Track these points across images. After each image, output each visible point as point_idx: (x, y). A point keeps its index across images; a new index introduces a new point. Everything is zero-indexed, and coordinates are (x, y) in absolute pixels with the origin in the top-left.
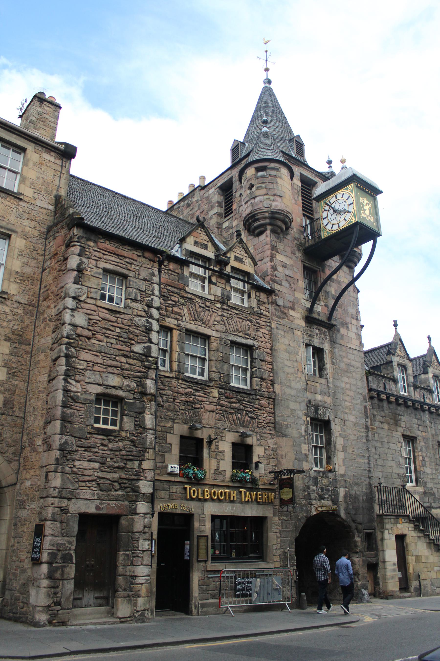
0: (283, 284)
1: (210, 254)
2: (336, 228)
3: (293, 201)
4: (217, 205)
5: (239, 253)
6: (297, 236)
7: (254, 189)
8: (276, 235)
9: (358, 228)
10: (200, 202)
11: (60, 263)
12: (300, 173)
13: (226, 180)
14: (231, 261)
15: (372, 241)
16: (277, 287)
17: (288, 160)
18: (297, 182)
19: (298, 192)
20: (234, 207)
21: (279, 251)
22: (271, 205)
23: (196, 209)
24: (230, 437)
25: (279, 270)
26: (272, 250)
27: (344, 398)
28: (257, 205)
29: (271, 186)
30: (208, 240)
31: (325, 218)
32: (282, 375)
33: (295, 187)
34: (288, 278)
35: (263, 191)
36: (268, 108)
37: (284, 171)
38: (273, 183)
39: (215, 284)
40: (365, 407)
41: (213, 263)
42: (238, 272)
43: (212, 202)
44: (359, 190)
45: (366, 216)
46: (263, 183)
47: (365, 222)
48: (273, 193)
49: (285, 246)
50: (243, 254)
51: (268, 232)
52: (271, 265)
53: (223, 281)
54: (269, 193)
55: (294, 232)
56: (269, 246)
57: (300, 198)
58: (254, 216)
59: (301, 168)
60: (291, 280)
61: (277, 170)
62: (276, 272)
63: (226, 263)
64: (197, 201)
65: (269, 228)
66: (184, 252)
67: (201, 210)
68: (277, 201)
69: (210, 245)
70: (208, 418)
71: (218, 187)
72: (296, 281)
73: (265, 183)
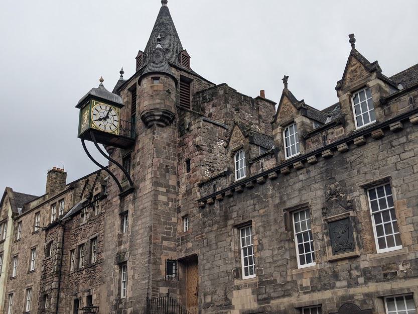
24: (86, 294)
27: (137, 238)
32: (106, 245)
36: (164, 25)
40: (151, 236)
70: (81, 288)
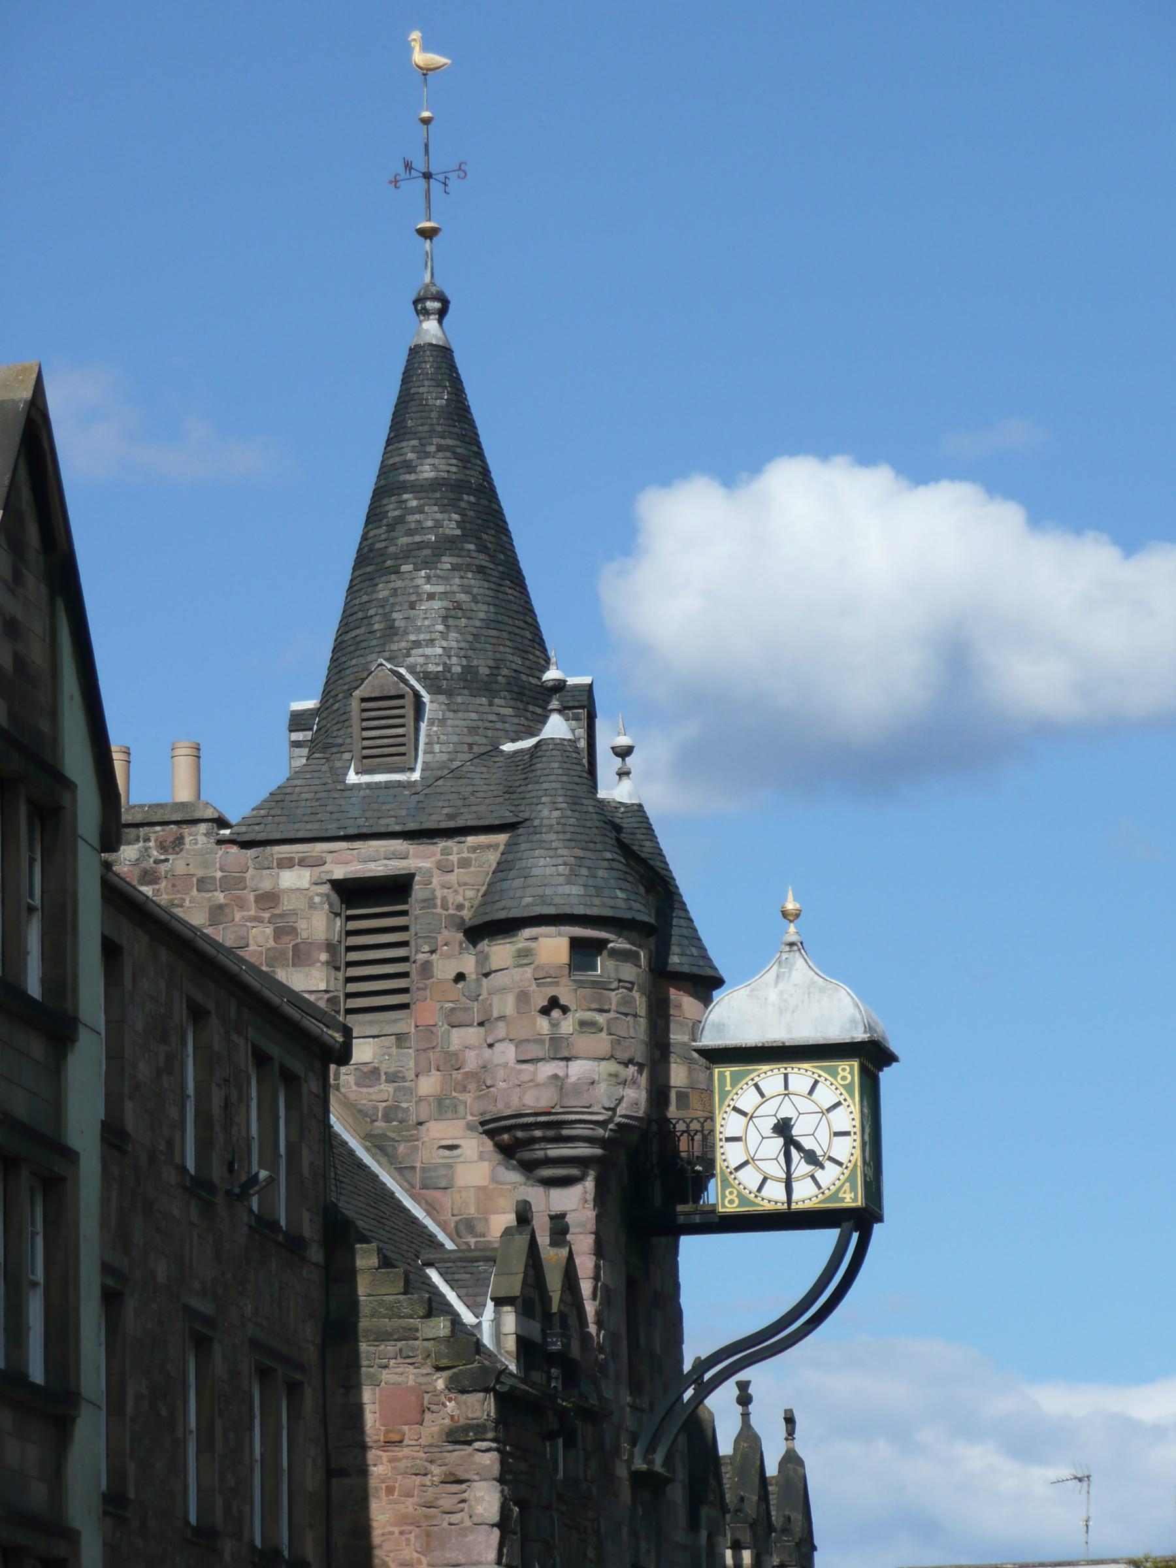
4: (324, 957)
7: (567, 1025)
10: (220, 897)
11: (427, 1480)
20: (428, 1010)
38: (626, 1015)
43: (293, 931)
46: (601, 1011)
48: (626, 1056)
51: (589, 1184)
54: (619, 1054)
64: (203, 884)
66: (510, 1344)
73: (608, 1011)
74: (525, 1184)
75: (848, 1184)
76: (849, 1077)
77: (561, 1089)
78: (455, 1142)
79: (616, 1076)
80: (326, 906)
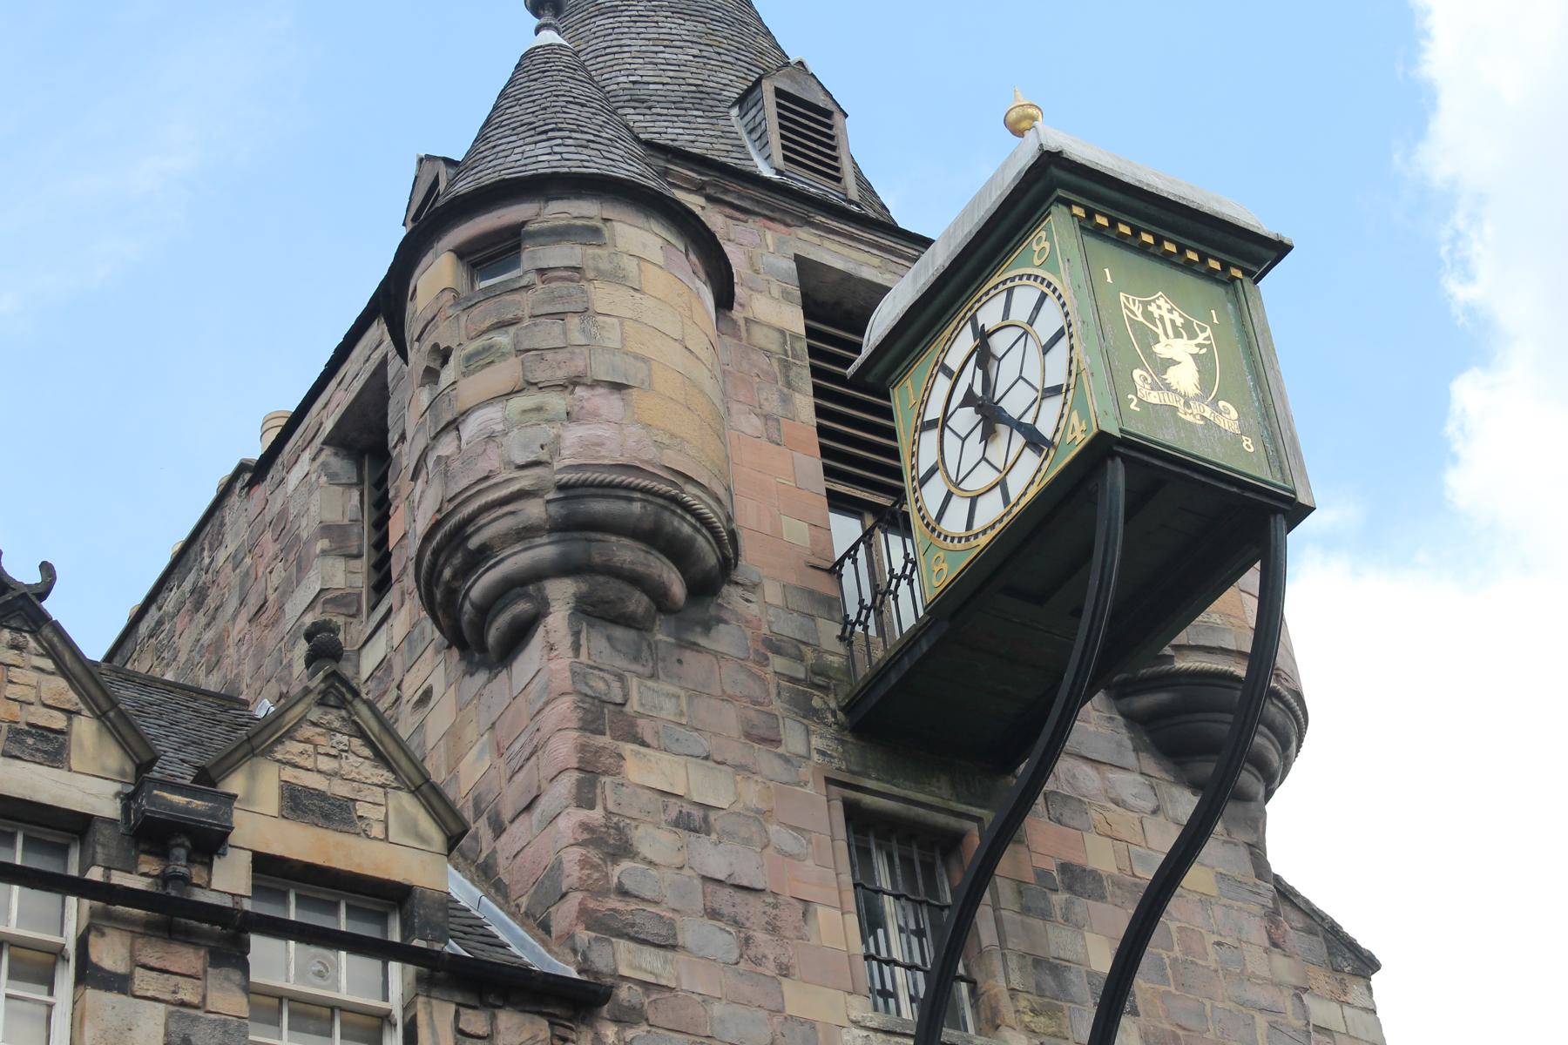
0: (685, 937)
1: (88, 784)
2: (991, 510)
3: (750, 424)
5: (325, 764)
6: (789, 627)
7: (448, 375)
8: (619, 632)
9: (1117, 475)
12: (798, 259)
13: (357, 385)
14: (239, 818)
15: (1258, 565)
16: (628, 961)
17: (699, 189)
18: (777, 313)
19: (786, 366)
21: (645, 728)
22: (555, 446)
23: (233, 603)
25: (645, 850)
26: (592, 724)
28: (468, 462)
29: (547, 334)
30: (71, 698)
31: (932, 471)
33: (770, 341)
34: (724, 899)
35: (504, 374)
37: (639, 239)
38: (560, 316)
39: (118, 983)
41: (105, 844)
42: (324, 894)
44: (1093, 243)
45: (1170, 399)
46: (502, 325)
47: (1167, 436)
48: (560, 375)
49: (695, 694)
50: (352, 771)
52: (585, 826)
53: (188, 958)
54: (539, 375)
55: (764, 600)
56: (565, 705)
57: (805, 405)
58: (459, 534)
59: (804, 233)
60: (753, 909)
61: (591, 234)
62: (626, 864)
63: (209, 842)
65: (561, 593)
67: (253, 603)
68: (595, 415)
69: (85, 729)
71: (325, 443)
72: (789, 917)
74: (489, 681)
75: (1075, 418)
76: (1047, 245)
77: (446, 472)
78: (425, 686)
79: (539, 409)
80: (324, 479)
